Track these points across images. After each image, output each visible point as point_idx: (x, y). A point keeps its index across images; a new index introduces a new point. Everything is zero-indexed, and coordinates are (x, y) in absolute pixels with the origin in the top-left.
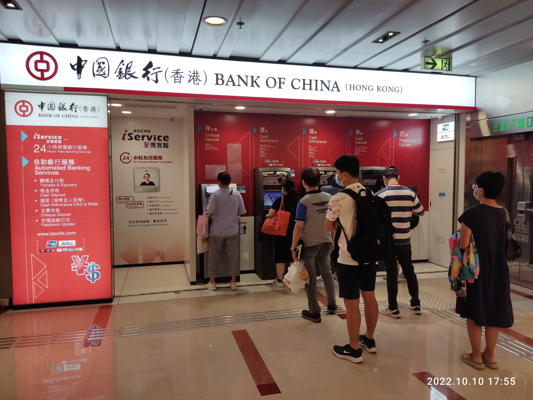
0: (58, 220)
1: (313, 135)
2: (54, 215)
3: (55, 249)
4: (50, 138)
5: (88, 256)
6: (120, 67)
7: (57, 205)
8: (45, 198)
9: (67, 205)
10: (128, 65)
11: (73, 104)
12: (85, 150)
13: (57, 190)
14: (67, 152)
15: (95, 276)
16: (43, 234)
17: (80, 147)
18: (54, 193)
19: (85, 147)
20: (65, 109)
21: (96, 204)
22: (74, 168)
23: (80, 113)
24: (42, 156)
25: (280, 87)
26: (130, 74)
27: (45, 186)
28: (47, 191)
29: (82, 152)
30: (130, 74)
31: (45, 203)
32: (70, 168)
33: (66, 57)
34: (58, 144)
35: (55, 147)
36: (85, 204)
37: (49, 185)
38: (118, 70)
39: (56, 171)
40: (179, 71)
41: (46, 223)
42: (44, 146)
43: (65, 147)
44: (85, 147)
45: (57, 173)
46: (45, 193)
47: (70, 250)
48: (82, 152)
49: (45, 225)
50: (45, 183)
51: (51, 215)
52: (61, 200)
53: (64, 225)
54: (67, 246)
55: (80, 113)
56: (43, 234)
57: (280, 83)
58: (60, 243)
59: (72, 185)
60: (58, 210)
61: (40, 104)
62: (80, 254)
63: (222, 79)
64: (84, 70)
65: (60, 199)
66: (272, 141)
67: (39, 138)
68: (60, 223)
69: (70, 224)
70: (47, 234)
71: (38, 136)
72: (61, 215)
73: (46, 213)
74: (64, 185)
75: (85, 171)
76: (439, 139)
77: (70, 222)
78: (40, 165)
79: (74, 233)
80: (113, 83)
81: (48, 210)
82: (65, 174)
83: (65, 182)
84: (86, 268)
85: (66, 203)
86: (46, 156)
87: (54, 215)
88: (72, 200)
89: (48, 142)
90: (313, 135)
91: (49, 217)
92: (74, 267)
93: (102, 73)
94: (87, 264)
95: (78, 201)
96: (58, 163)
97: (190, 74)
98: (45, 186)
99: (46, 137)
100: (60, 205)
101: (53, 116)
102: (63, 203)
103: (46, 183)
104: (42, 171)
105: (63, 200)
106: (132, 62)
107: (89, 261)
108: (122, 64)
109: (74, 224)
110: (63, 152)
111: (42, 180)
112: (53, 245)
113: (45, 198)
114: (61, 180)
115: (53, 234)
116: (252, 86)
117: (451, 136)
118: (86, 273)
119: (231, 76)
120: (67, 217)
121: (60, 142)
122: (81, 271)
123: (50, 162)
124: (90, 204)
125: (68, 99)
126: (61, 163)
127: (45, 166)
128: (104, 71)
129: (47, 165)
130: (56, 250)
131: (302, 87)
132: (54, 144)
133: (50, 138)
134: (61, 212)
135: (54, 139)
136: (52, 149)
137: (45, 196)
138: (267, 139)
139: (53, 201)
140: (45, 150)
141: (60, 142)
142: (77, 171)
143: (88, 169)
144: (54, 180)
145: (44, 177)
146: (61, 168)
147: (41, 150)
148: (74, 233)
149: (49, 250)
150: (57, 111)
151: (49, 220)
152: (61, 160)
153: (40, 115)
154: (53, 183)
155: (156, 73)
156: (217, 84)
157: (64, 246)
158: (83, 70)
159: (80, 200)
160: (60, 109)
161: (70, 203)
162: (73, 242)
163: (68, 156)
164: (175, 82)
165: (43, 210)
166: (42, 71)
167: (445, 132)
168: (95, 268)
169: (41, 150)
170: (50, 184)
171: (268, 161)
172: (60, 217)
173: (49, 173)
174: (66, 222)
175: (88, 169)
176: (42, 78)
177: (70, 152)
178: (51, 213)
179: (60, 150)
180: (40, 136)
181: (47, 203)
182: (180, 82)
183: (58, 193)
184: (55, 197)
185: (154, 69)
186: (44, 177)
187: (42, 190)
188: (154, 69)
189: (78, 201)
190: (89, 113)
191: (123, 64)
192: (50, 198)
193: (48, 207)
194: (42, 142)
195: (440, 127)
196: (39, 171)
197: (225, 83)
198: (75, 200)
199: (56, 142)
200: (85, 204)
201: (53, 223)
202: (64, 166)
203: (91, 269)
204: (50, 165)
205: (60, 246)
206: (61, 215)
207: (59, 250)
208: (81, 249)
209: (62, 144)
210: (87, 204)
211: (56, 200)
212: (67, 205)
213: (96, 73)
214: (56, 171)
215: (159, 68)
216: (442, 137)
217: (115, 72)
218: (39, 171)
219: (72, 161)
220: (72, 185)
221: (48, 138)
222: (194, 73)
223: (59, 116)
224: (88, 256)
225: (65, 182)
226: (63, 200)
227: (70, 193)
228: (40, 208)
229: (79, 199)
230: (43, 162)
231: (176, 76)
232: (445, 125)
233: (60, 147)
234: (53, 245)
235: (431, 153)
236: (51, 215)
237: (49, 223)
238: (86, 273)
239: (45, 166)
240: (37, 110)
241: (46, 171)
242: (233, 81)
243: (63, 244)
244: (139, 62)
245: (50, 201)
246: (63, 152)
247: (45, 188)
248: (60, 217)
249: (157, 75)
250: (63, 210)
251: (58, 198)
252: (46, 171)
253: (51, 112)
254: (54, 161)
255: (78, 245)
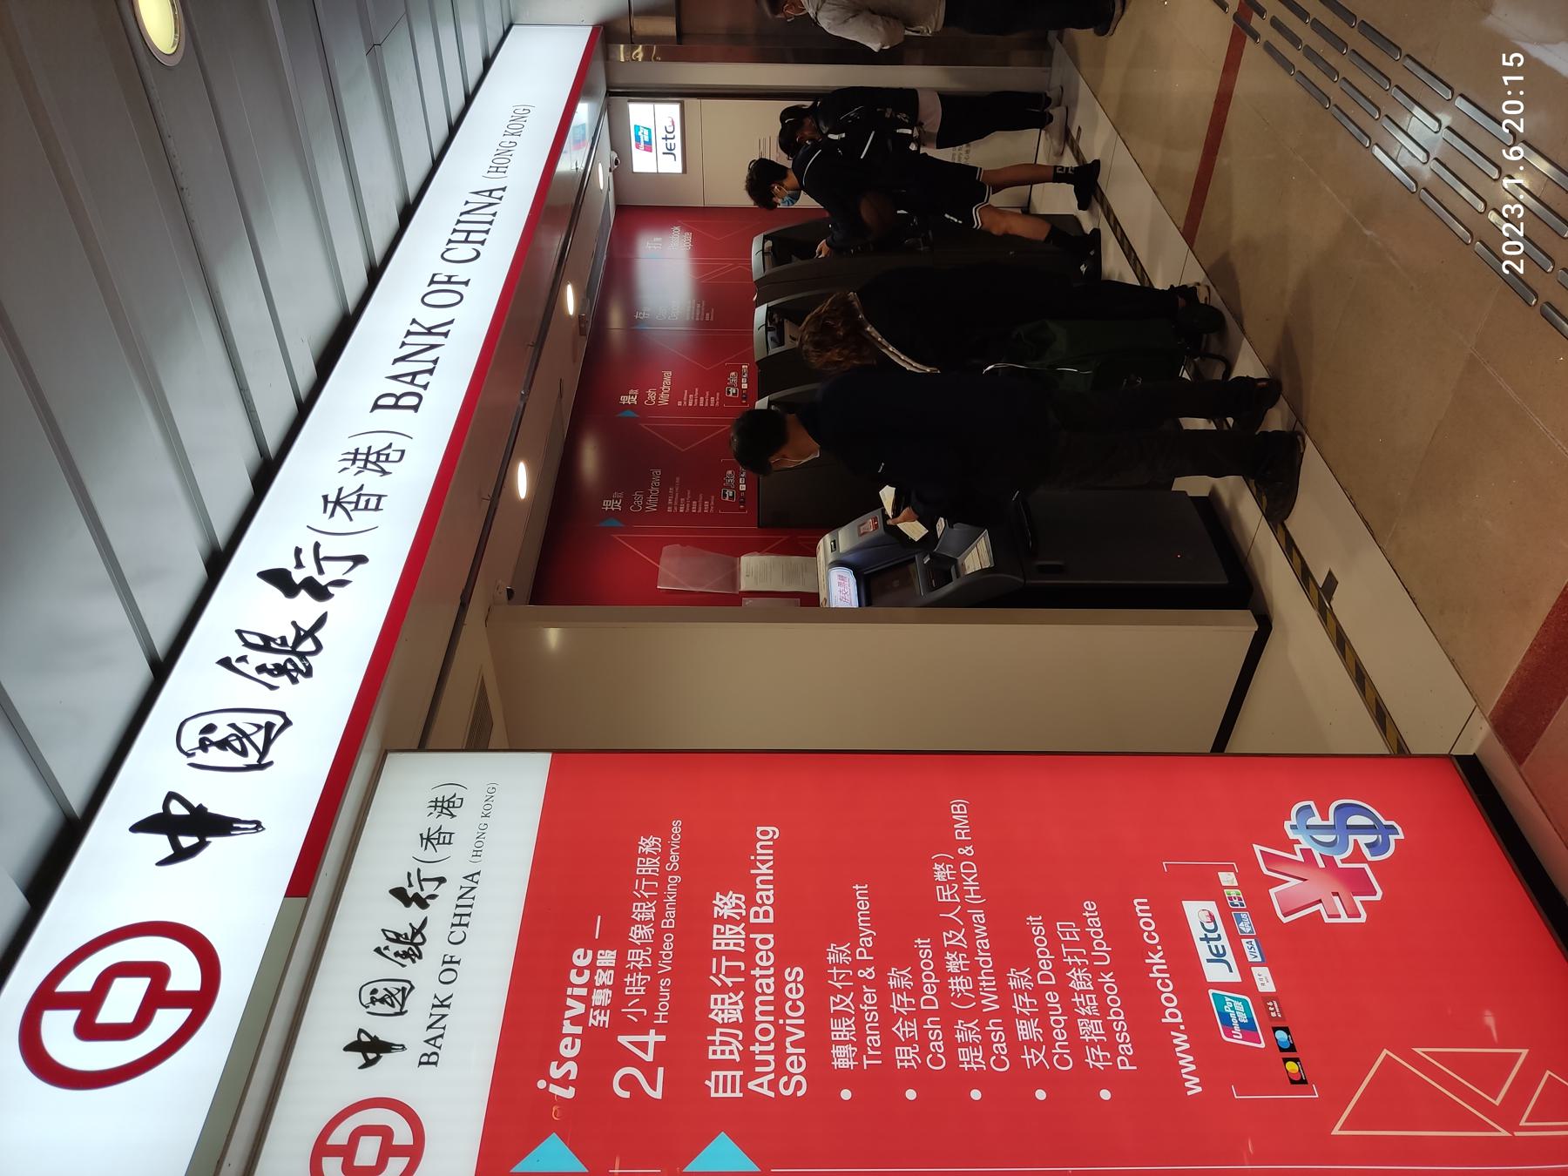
0: (1079, 980)
1: (642, 397)
2: (1052, 999)
3: (1262, 1000)
4: (580, 1008)
5: (1257, 848)
6: (254, 674)
7: (987, 982)
8: (952, 1046)
9: (981, 931)
10: (247, 644)
11: (399, 893)
12: (666, 846)
13: (898, 978)
14: (669, 922)
15: (1355, 820)
16: (1187, 1063)
17: (647, 867)
18: (916, 991)
19: (648, 844)
20: (417, 932)
21: (959, 810)
22: (766, 894)
23: (454, 863)
24: (686, 1052)
25: (466, 283)
26: (299, 639)
27: (874, 1038)
28: (903, 1029)
29: (674, 858)
30: (299, 639)
31: (987, 1044)
32: (764, 912)
33: (117, 877)
34: (621, 970)
35: (636, 985)
36: (962, 851)
37: (872, 1018)
38: (265, 677)
39: (781, 983)
40: (332, 498)
41: (1110, 1046)
42: (624, 1040)
43: (639, 933)
44: (648, 844)
45: (794, 974)
46: (924, 1042)
47: (1246, 926)
48: (674, 858)
49: (1126, 1047)
50: (860, 1043)
51: (1057, 1017)
52: (954, 963)
53: (1102, 948)
54: (1225, 941)
55: (454, 863)
56: (1187, 1063)
57: (449, 282)
58: (1215, 973)
59: (863, 906)
60: (1018, 979)
61: (358, 1058)
62: (1256, 887)
63: (398, 398)
64: (217, 807)
65: (952, 967)
66: (656, 481)
67: (572, 1067)
68: (1095, 972)
69: (1094, 924)
70: (1181, 1040)
71: (555, 1073)
72: (1045, 967)
73: (1050, 1042)
74: (866, 941)
75: (777, 846)
76: (672, 166)
77: (1082, 922)
78: (748, 1064)
79: (1140, 906)
80: (322, 705)
81: (1027, 1030)
82: (802, 934)
83: (850, 935)
84: (1329, 860)
85: (971, 936)
86: (689, 1027)
87: (1052, 999)
88: (950, 907)
89: (600, 1019)
90: (642, 397)
91: (1071, 1027)
92: (1339, 911)
93: (259, 739)
94: (1307, 853)
95: (953, 880)
96: (731, 972)
97: (354, 469)
98: (874, 1038)
99: (568, 1028)
100: (988, 968)
101: (443, 992)
102: (971, 952)
103: (861, 1034)
104: (780, 1054)
105: (952, 949)
106: (239, 632)
107: (1289, 845)
108: (241, 666)
109: (1089, 906)
110: (668, 946)
111: (843, 1058)
112: (1238, 1009)
113: (952, 1046)
114: (837, 954)
115: (1171, 1007)
116: (446, 335)
117: (668, 113)
118: (1357, 856)
119: (395, 378)
120: (1051, 935)
121: (608, 958)
122: (1355, 882)
123: (726, 1009)
124: (961, 830)
125: (366, 912)
126: (731, 955)
127: (749, 1040)
128: (249, 730)
129: (747, 1024)
130: (1267, 997)
131: (478, 246)
132: (618, 987)
133: (580, 1008)
134: (1027, 959)
135: (590, 986)
136: (651, 998)
137: (937, 1045)
138: (647, 495)
139: (964, 1000)
140: (652, 1038)
141: (608, 958)
142: (777, 882)
143: (767, 834)
144: (835, 991)
145: (818, 1044)
146: (765, 956)
147: (649, 1057)
148: (1140, 906)
149: (1281, 1035)
150: (424, 973)
151: (1090, 1029)
152: (719, 954)
153: (427, 1061)
154: (858, 1000)
155: (317, 560)
156: (415, 408)
157: (1230, 957)
158: (213, 809)
159: (941, 873)
160: (413, 954)
161: (964, 915)
162: (1197, 912)
163: (695, 922)
164: (377, 509)
165: (1031, 1057)
166: (158, 998)
167: (657, 137)
168: (1316, 820)
169: (649, 1057)
170: (860, 1014)
171: (729, 493)
172: (1060, 969)
173: (795, 1018)
174: (1086, 940)
175: (767, 834)
176: (200, 1003)
177: (671, 913)
178: (1042, 1014)
179: (656, 956)
180: (562, 1061)
181: (986, 1035)
182: (380, 497)
183: (916, 973)
184: (943, 991)
185: (299, 565)
186: (818, 1044)
187: (906, 1057)
188: (299, 565)
189: (953, 880)
190: (462, 825)
191: (243, 659)
192: (948, 1018)
193: (1011, 1031)
194: (601, 1052)
195: (642, 162)
196: (780, 1070)
197: (420, 390)
198: (945, 895)
199: (604, 978)
200: (962, 851)
201: (1104, 1009)
202: (750, 943)
203: (1329, 838)
204: (748, 1011)
205: (1235, 977)
206: (1045, 967)
207: (1264, 981)
208: (1227, 878)
209: (621, 944)
210: (964, 844)
211: (959, 985)
212: (981, 931)
213: (253, 757)
214: (781, 983)
215: (298, 551)
216: (670, 151)
217: (272, 687)
218: (780, 1070)
219: (726, 904)
220: (863, 906)
221: (575, 1021)
222: (354, 461)
223: (450, 963)
224: (1257, 848)
225: (850, 935)
226: (952, 949)
227: (909, 922)
228: (1026, 1078)
229: (939, 876)
230: (724, 1047)
231: (350, 507)
232: (638, 139)
233: (637, 958)
234: (1238, 1009)
235: (711, 203)
236: (1057, 1017)
237: (1108, 1026)
238: (1357, 856)
239: (749, 1040)
240: (389, 1077)
241: (782, 1033)
242: (414, 374)
243: (1219, 957)
244: (244, 603)
245: (968, 1016)
246: (668, 946)
247: (890, 1041)
248: (1060, 969)
249: (327, 558)
250: (1012, 950)
251: (942, 972)
252: (782, 1033)
253: (419, 1005)
254: (724, 989)
255: (1212, 891)
